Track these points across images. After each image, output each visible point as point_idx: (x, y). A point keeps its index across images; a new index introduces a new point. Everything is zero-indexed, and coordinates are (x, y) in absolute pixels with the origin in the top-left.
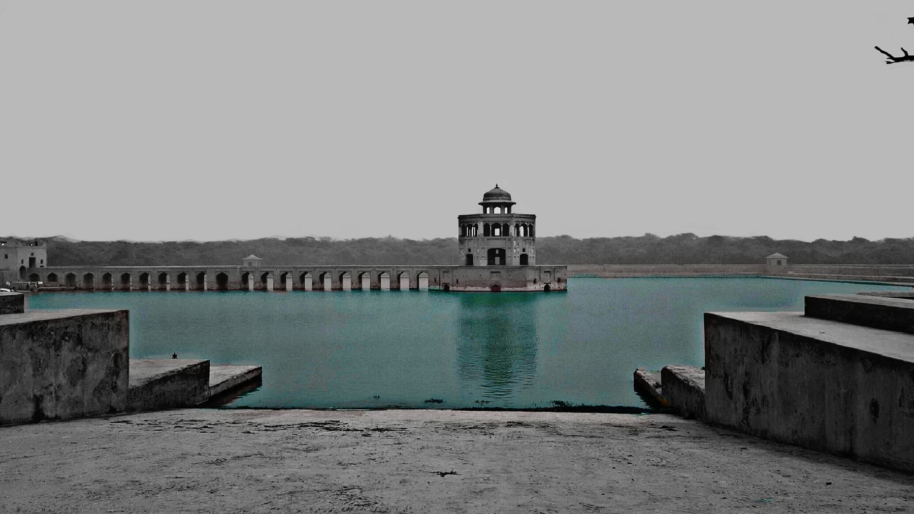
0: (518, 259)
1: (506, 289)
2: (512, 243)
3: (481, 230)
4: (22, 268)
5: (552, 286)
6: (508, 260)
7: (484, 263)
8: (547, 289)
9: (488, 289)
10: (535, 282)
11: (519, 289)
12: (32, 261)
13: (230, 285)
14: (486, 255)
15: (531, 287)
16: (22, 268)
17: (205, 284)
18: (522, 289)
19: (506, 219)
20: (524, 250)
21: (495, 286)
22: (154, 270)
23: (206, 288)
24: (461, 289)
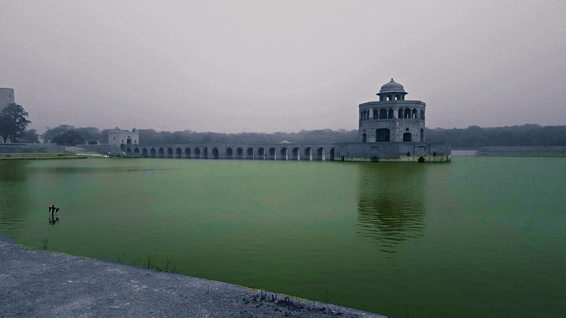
0: (402, 137)
1: (383, 160)
2: (395, 124)
3: (371, 115)
4: (122, 145)
5: (426, 159)
6: (391, 138)
7: (373, 140)
8: (421, 160)
9: (368, 160)
10: (408, 155)
11: (393, 160)
12: (129, 141)
13: (220, 156)
14: (375, 134)
15: (404, 159)
16: (122, 145)
17: (287, 156)
18: (396, 160)
19: (391, 105)
20: (407, 130)
21: (375, 157)
22: (174, 148)
23: (287, 158)
24: (350, 159)
